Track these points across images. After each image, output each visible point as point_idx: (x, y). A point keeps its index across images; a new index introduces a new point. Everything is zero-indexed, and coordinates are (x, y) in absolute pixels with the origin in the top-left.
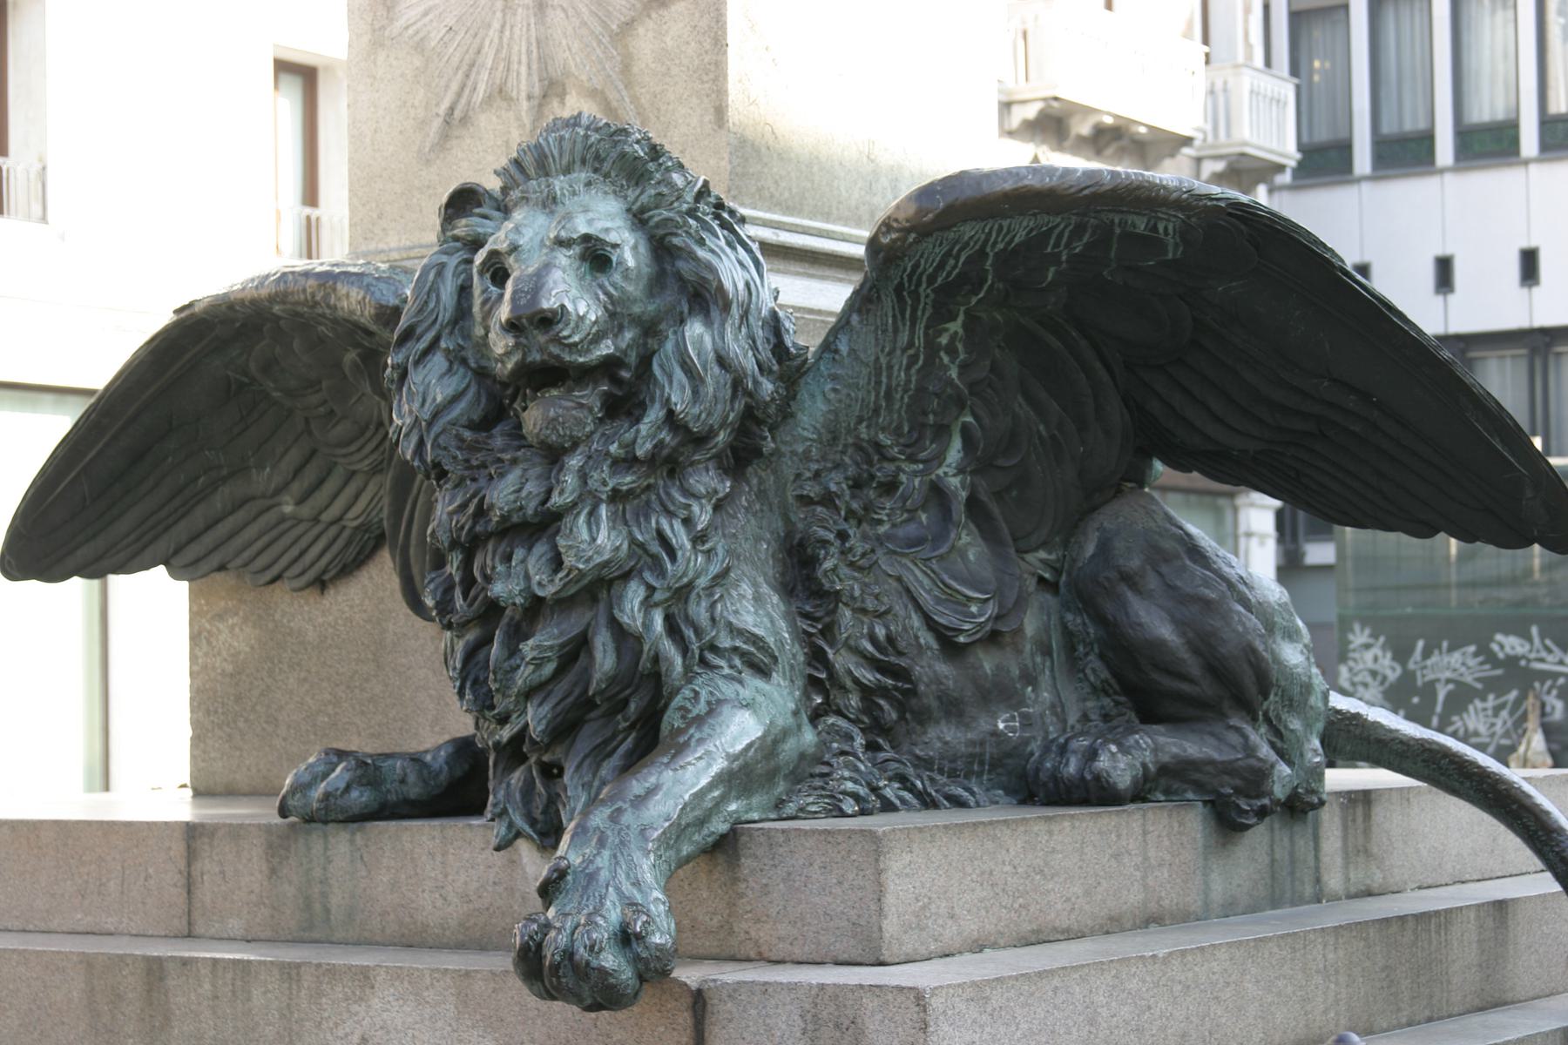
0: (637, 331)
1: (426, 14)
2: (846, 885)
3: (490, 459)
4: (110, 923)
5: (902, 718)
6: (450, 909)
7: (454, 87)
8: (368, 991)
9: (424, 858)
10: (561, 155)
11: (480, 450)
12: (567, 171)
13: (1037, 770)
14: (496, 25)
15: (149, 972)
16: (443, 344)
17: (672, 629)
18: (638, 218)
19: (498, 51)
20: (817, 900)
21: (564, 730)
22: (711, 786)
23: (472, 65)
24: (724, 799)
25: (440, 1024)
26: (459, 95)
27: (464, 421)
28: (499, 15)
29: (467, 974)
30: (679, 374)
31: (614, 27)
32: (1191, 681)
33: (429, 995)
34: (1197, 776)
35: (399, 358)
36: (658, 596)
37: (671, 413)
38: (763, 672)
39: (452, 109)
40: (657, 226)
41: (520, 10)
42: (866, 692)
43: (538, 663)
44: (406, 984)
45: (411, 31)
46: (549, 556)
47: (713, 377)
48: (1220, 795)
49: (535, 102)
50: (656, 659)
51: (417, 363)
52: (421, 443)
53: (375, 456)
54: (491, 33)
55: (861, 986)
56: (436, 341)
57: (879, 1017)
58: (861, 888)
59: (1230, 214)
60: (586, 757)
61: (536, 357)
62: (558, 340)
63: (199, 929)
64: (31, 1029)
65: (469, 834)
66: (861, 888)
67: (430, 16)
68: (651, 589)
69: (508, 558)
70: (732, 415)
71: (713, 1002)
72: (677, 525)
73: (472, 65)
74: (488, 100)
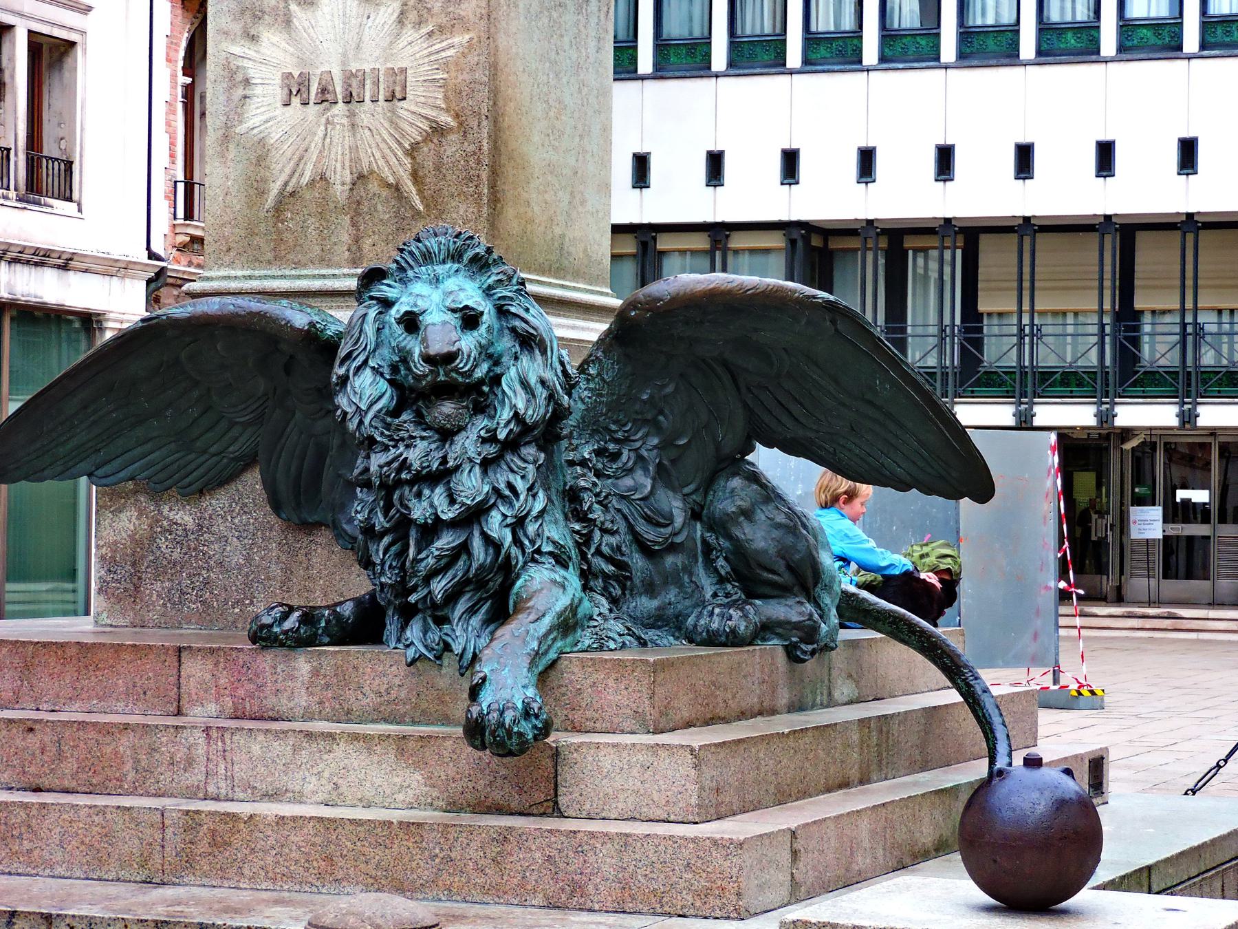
0: (491, 362)
1: (267, 121)
2: (630, 690)
3: (406, 435)
5: (624, 593)
6: (365, 701)
7: (288, 171)
8: (335, 746)
9: (350, 670)
10: (439, 253)
11: (400, 430)
13: (695, 626)
14: (320, 133)
16: (371, 363)
17: (517, 541)
19: (320, 152)
20: (612, 698)
21: (452, 597)
22: (549, 632)
23: (301, 159)
24: (554, 640)
25: (384, 766)
26: (291, 176)
27: (384, 412)
28: (323, 128)
29: (404, 737)
31: (407, 146)
32: (779, 575)
33: (378, 749)
34: (780, 630)
35: (342, 371)
37: (516, 414)
38: (566, 567)
39: (286, 184)
40: (500, 298)
41: (338, 127)
42: (606, 576)
43: (439, 558)
44: (362, 743)
45: (255, 131)
46: (445, 494)
47: (541, 393)
48: (791, 642)
49: (347, 187)
50: (508, 557)
51: (355, 374)
52: (361, 422)
53: (252, 415)
54: (316, 139)
55: (658, 745)
56: (365, 362)
57: (668, 761)
58: (639, 691)
59: (824, 307)
60: (463, 614)
61: (442, 378)
62: (456, 370)
64: (87, 769)
65: (382, 657)
66: (639, 691)
67: (271, 123)
68: (505, 516)
69: (419, 495)
70: (548, 415)
71: (564, 753)
72: (518, 478)
73: (301, 159)
74: (312, 183)
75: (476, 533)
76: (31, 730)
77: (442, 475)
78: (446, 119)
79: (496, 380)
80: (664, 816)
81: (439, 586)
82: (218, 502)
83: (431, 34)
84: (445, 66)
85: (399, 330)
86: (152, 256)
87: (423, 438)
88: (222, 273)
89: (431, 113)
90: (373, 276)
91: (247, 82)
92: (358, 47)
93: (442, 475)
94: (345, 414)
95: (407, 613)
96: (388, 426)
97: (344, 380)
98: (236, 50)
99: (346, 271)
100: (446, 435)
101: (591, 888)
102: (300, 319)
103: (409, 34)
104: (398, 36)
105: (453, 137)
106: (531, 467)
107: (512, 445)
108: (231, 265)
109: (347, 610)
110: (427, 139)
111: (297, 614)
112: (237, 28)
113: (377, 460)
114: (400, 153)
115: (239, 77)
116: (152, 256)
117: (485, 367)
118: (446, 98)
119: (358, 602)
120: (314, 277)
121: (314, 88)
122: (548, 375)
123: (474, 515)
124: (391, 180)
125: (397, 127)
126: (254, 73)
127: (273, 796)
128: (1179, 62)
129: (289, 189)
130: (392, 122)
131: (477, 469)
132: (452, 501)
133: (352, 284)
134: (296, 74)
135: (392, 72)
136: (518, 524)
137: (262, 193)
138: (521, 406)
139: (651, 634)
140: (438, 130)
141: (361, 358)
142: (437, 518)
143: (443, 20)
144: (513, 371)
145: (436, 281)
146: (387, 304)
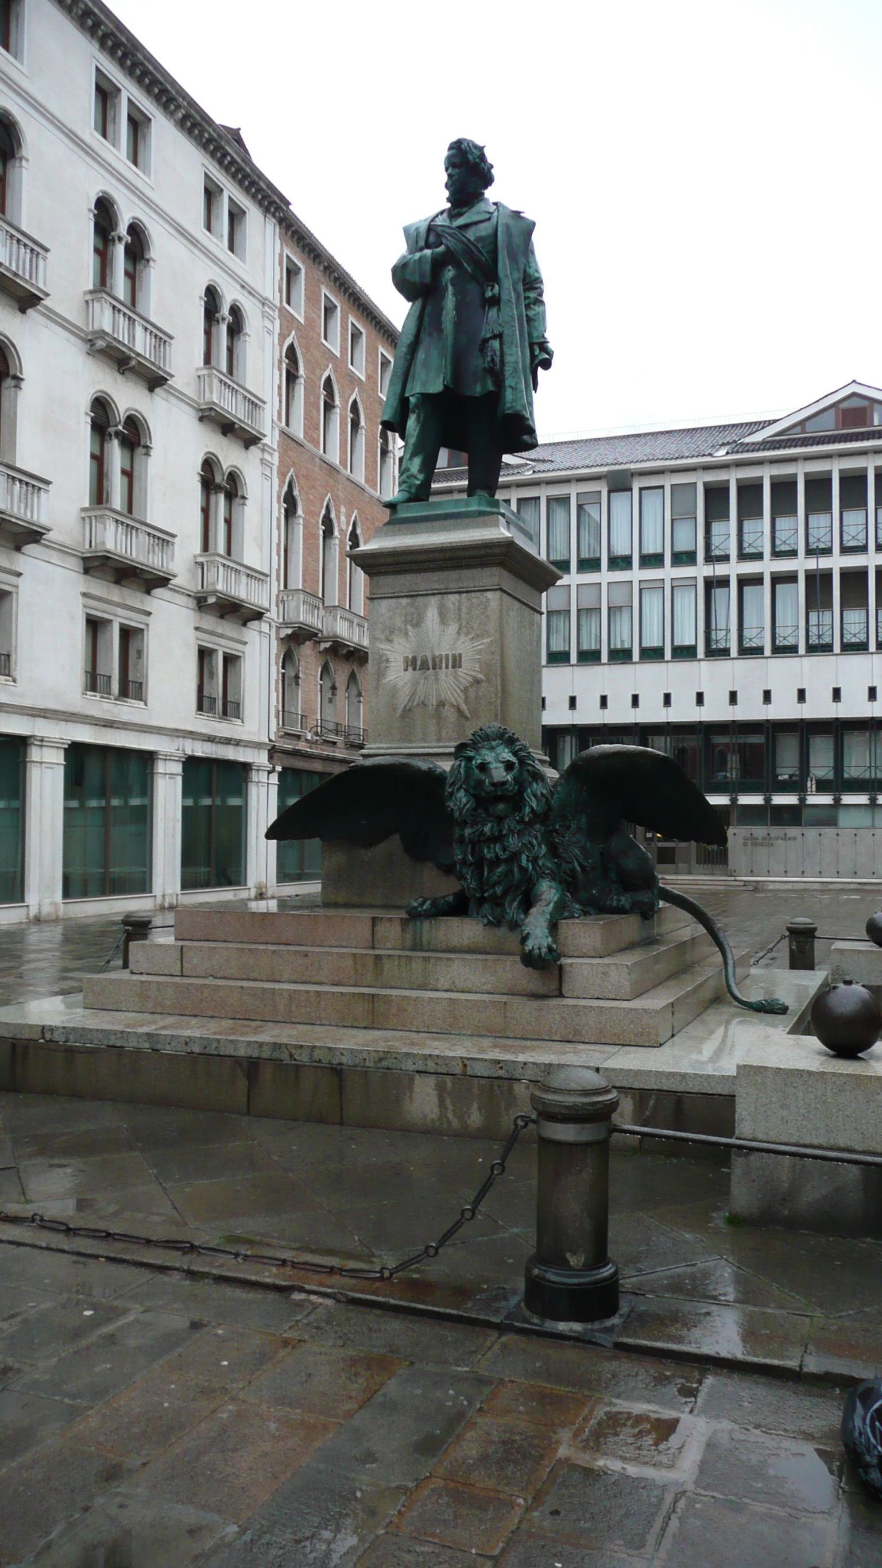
4: (344, 944)
12: (495, 740)
15: (376, 958)
18: (515, 754)
21: (505, 894)
26: (408, 702)
30: (533, 799)
35: (450, 790)
36: (530, 859)
39: (405, 707)
50: (531, 876)
61: (499, 793)
62: (506, 789)
63: (376, 946)
68: (528, 857)
69: (489, 847)
74: (418, 705)
75: (516, 865)
76: (306, 955)
77: (498, 838)
78: (481, 676)
79: (521, 792)
80: (614, 997)
81: (499, 890)
82: (382, 848)
83: (473, 638)
84: (480, 652)
85: (477, 771)
86: (270, 740)
87: (490, 821)
88: (377, 745)
89: (473, 673)
90: (461, 747)
91: (387, 661)
92: (439, 644)
93: (498, 838)
94: (452, 810)
95: (481, 901)
96: (473, 816)
97: (452, 794)
98: (383, 646)
99: (434, 744)
100: (500, 819)
101: (584, 1032)
102: (424, 765)
103: (463, 638)
104: (458, 640)
105: (484, 684)
106: (539, 834)
107: (530, 824)
108: (381, 742)
109: (451, 898)
110: (472, 685)
111: (429, 902)
112: (383, 637)
113: (467, 831)
114: (459, 691)
115: (384, 658)
116: (270, 740)
117: (517, 787)
118: (480, 666)
119: (455, 895)
120: (422, 748)
121: (419, 663)
122: (545, 792)
123: (515, 857)
124: (455, 703)
125: (458, 680)
126: (392, 657)
127: (423, 987)
128: (663, 664)
129: (408, 708)
130: (455, 678)
131: (516, 835)
132: (504, 849)
133: (453, 750)
134: (410, 657)
135: (454, 656)
136: (534, 860)
137: (395, 710)
138: (534, 806)
139: (589, 909)
140: (478, 682)
141: (460, 784)
142: (497, 857)
143: (479, 632)
144: (529, 790)
145: (492, 749)
146: (469, 759)
